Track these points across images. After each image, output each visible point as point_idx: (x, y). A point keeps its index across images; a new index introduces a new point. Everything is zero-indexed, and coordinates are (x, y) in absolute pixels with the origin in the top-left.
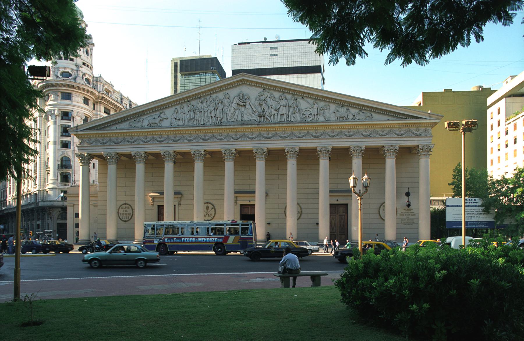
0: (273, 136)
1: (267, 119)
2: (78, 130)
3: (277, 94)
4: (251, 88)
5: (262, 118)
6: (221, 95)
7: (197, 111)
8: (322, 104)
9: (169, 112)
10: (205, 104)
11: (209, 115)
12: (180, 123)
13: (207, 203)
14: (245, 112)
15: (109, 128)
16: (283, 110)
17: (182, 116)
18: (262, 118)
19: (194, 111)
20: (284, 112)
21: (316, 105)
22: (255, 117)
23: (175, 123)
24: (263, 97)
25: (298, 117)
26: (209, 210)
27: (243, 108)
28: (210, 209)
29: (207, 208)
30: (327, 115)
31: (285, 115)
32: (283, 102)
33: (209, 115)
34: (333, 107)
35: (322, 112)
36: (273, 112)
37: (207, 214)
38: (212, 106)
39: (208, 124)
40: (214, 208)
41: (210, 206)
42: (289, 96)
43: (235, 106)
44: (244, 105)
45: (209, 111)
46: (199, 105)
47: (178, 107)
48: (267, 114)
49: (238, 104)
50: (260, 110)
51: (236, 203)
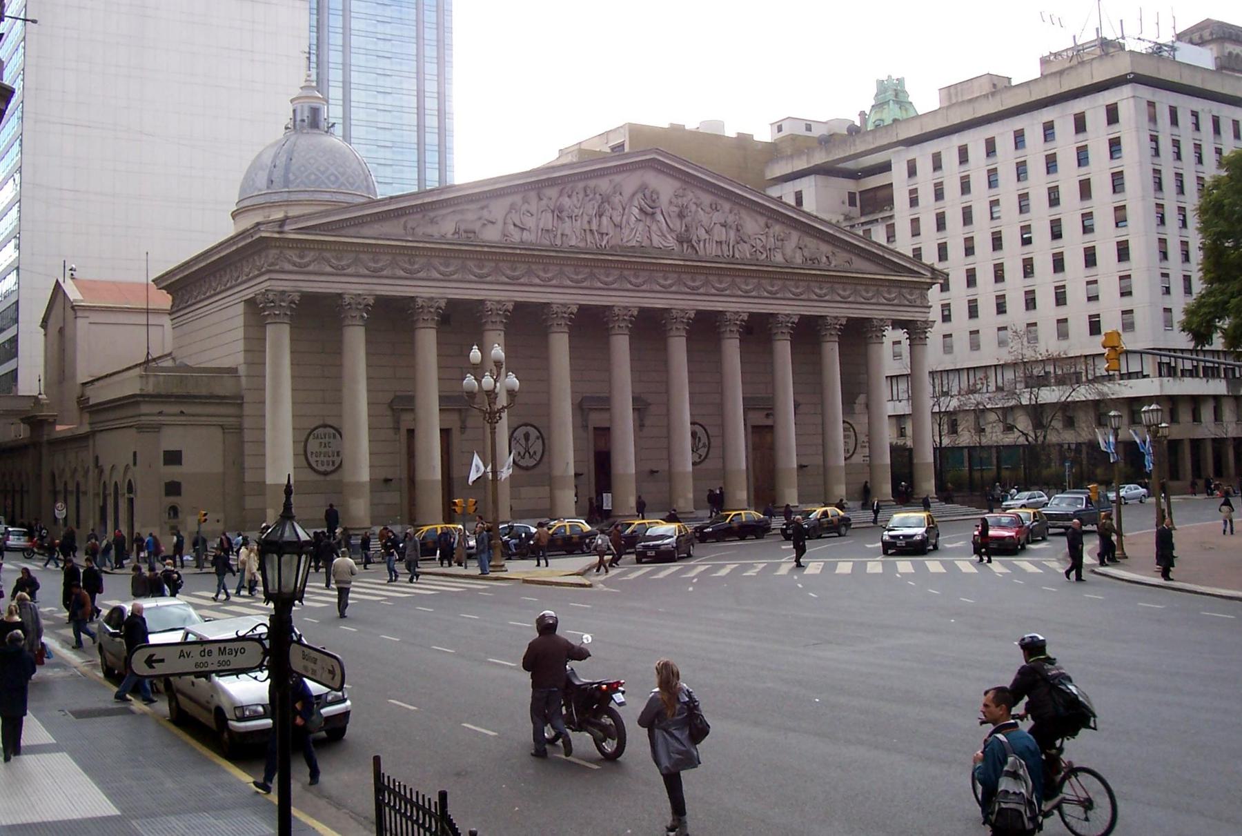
0: (702, 286)
1: (693, 246)
2: (287, 228)
3: (706, 199)
4: (661, 176)
5: (685, 246)
6: (604, 185)
7: (565, 214)
8: (777, 228)
9: (498, 209)
10: (574, 199)
11: (587, 227)
12: (526, 236)
13: (526, 425)
14: (654, 227)
15: (352, 231)
16: (719, 233)
17: (530, 222)
18: (685, 246)
19: (558, 213)
20: (724, 238)
21: (771, 231)
22: (671, 242)
23: (516, 236)
24: (685, 201)
25: (745, 251)
26: (530, 443)
27: (648, 219)
28: (532, 438)
29: (527, 437)
30: (789, 252)
31: (725, 247)
32: (717, 217)
33: (587, 227)
34: (795, 235)
35: (779, 243)
36: (703, 234)
37: (527, 451)
38: (591, 209)
39: (582, 245)
40: (541, 437)
41: (534, 433)
42: (727, 206)
43: (636, 211)
44: (653, 214)
45: (586, 218)
46: (566, 201)
47: (517, 198)
48: (695, 238)
49: (641, 209)
50: (677, 225)
51: (585, 427)
